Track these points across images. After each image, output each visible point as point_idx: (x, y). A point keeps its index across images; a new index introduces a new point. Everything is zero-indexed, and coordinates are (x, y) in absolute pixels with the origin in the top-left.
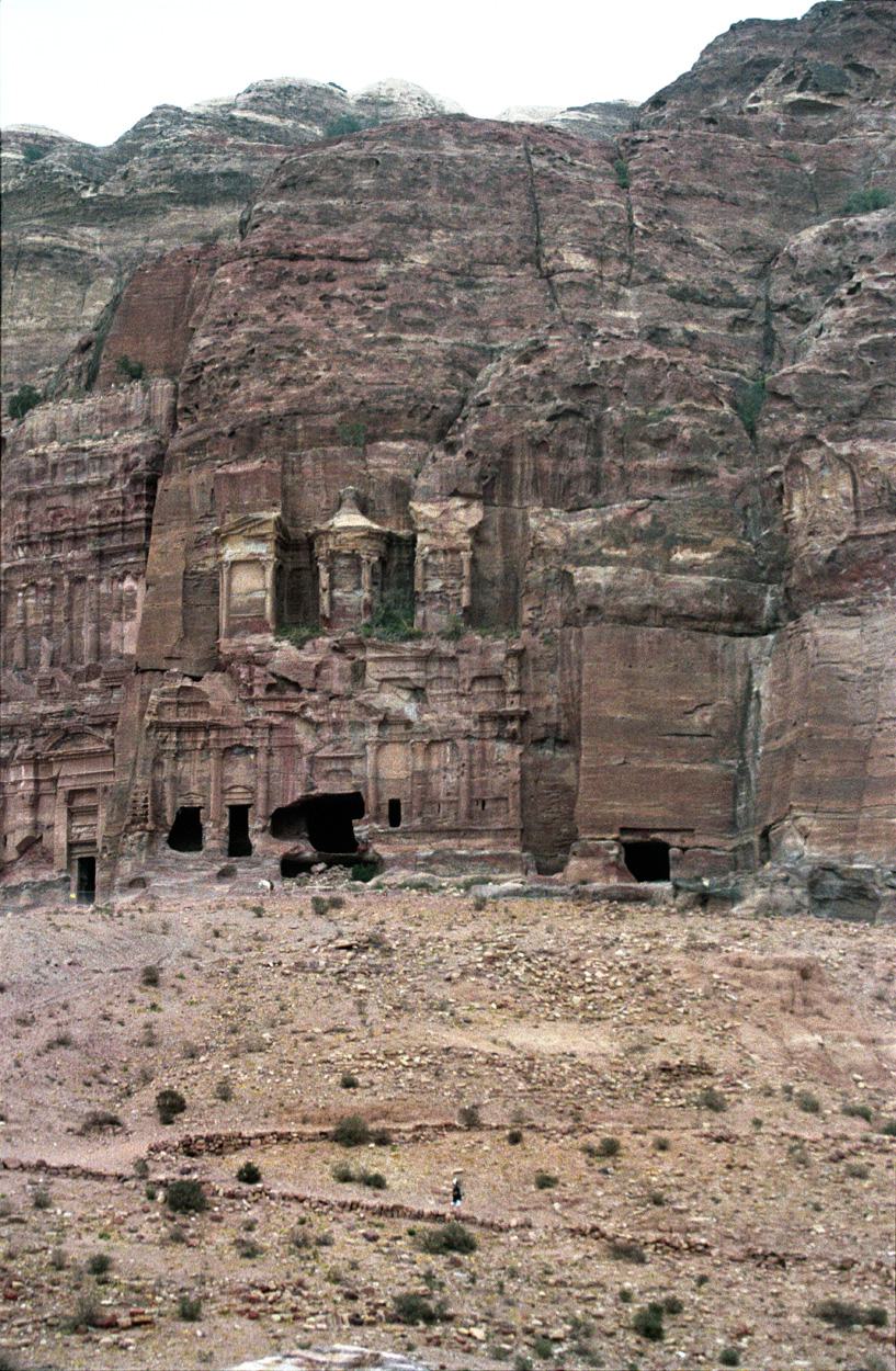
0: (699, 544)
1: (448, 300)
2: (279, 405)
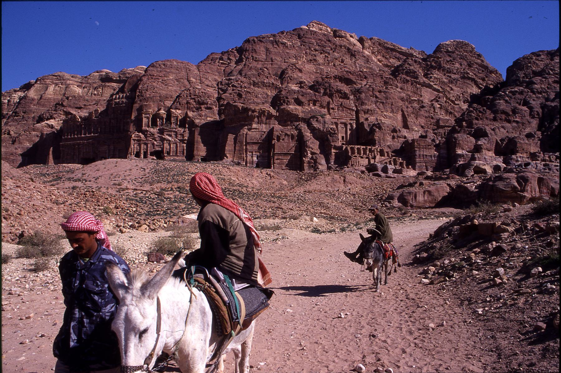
0: (211, 117)
2: (152, 96)
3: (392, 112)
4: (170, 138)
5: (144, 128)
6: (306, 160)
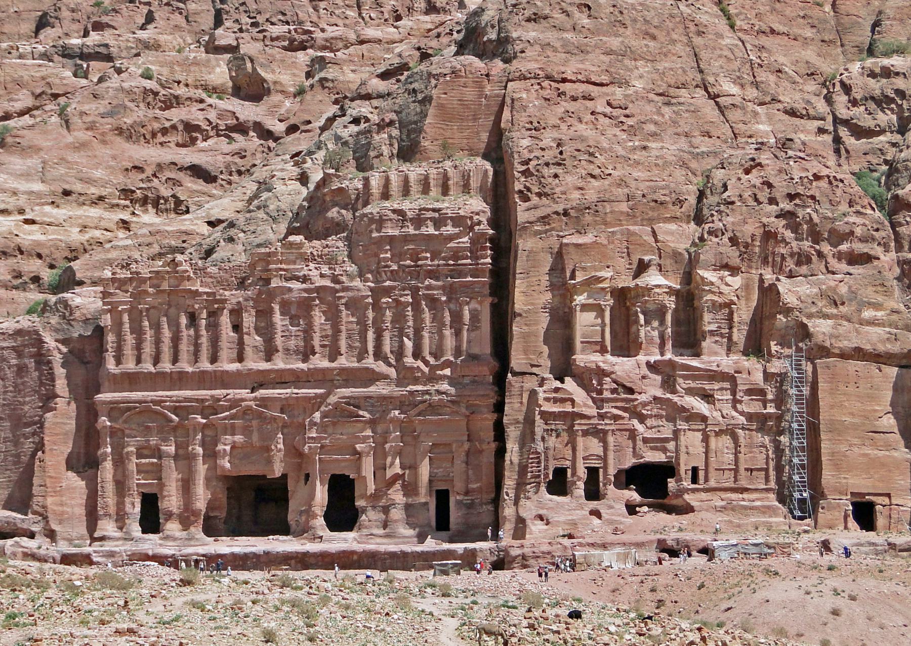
0: (877, 306)
1: (663, 116)
2: (592, 196)
4: (702, 407)
5: (584, 358)
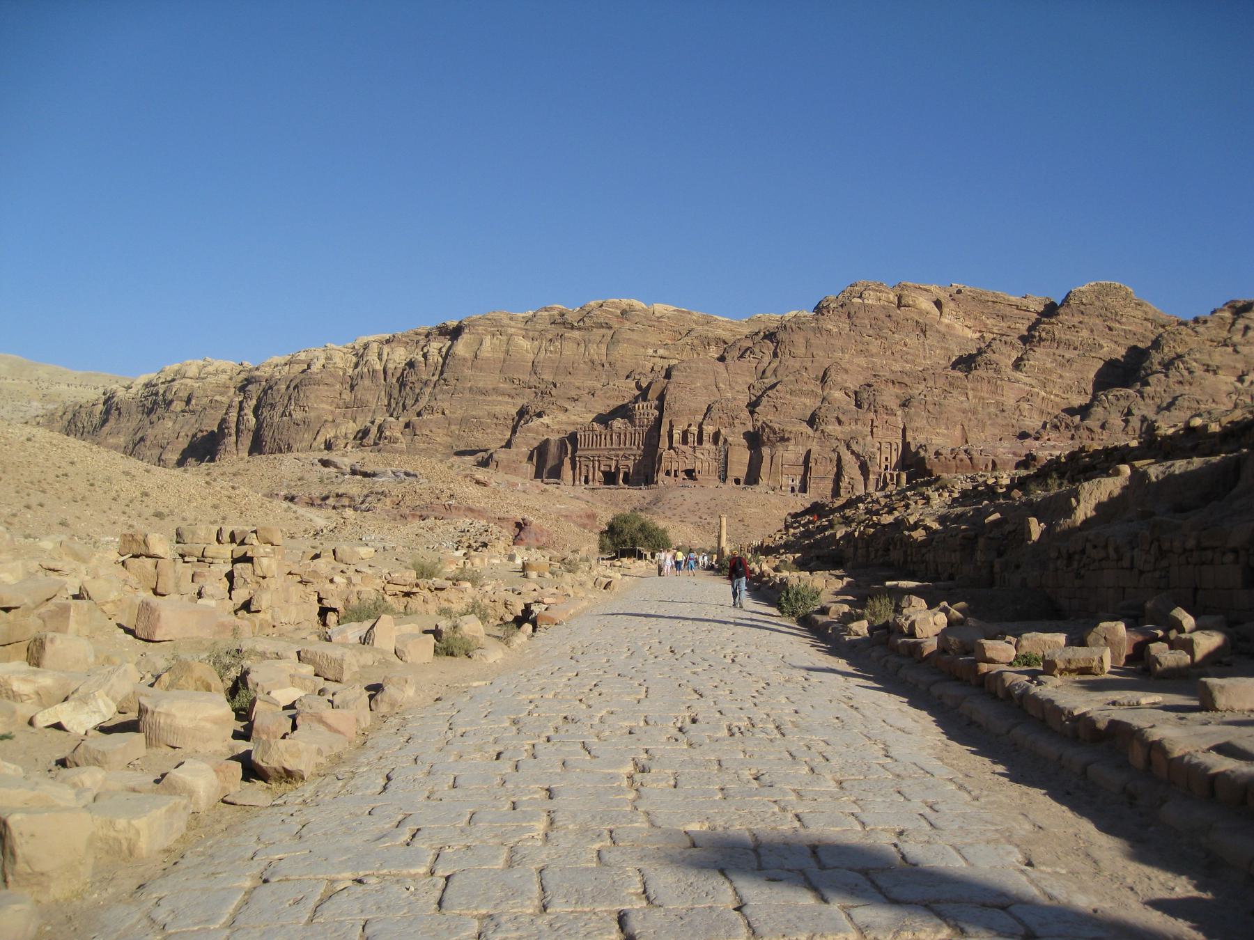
3: (947, 428)
6: (843, 485)
